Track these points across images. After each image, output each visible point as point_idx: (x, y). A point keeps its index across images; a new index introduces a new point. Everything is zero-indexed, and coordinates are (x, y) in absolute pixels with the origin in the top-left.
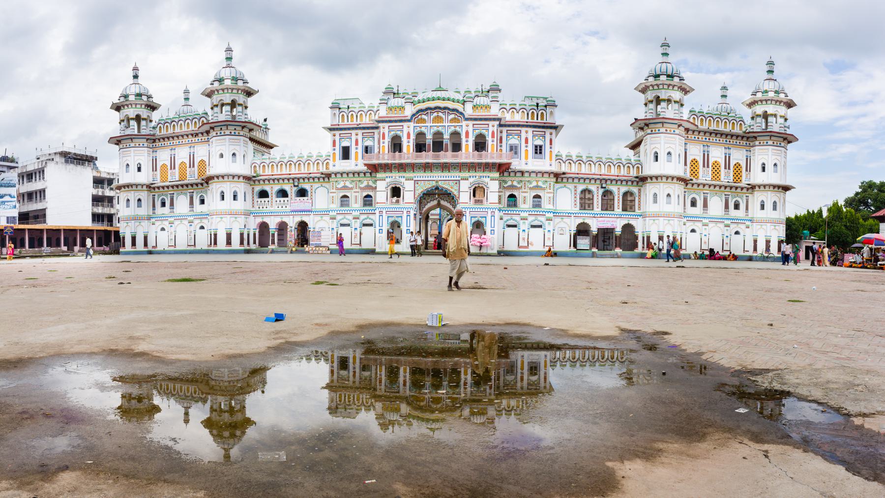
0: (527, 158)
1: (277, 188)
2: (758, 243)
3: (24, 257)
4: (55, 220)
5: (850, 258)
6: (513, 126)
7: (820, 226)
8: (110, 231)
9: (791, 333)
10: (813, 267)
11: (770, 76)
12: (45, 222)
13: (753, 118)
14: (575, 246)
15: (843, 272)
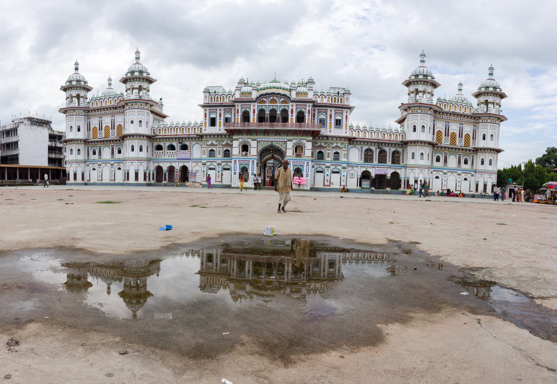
0: (330, 127)
1: (168, 144)
2: (487, 187)
3: (4, 185)
4: (24, 161)
5: (538, 197)
6: (322, 106)
7: (520, 176)
8: (60, 170)
9: (498, 245)
10: (514, 203)
11: (491, 77)
12: (18, 163)
13: (478, 105)
14: (360, 185)
15: (533, 206)
